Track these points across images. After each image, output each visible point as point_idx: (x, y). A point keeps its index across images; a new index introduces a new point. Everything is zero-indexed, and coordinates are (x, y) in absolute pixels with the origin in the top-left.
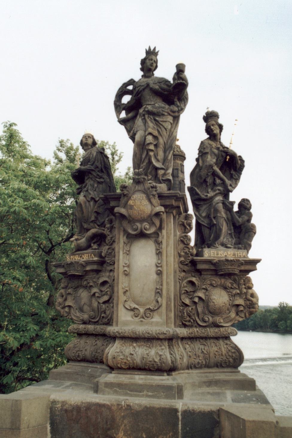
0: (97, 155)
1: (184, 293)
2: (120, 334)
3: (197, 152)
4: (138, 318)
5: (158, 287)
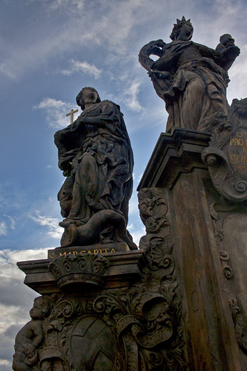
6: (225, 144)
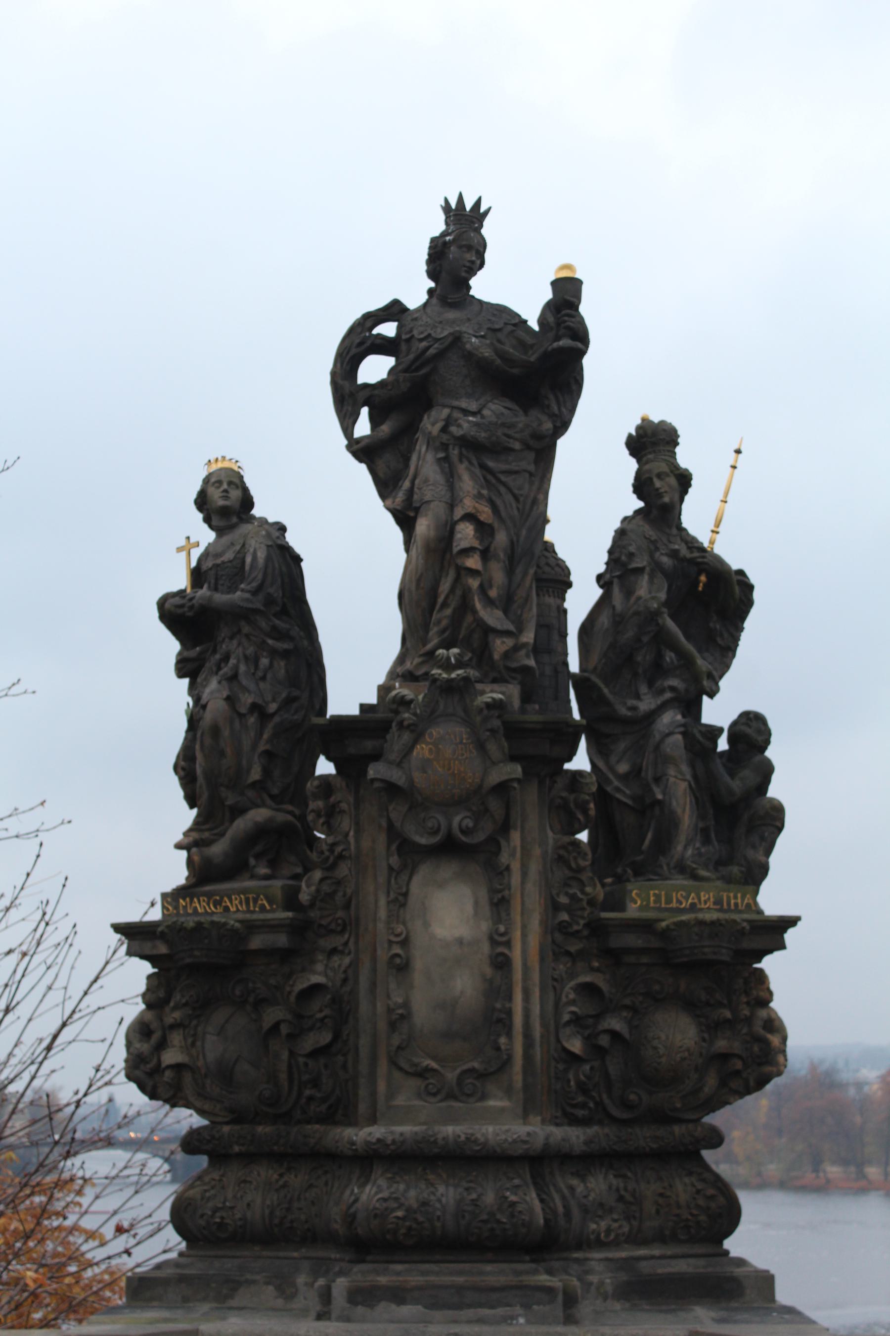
0: (268, 559)
1: (568, 1023)
2: (388, 1145)
3: (605, 557)
4: (439, 1097)
5: (498, 1005)
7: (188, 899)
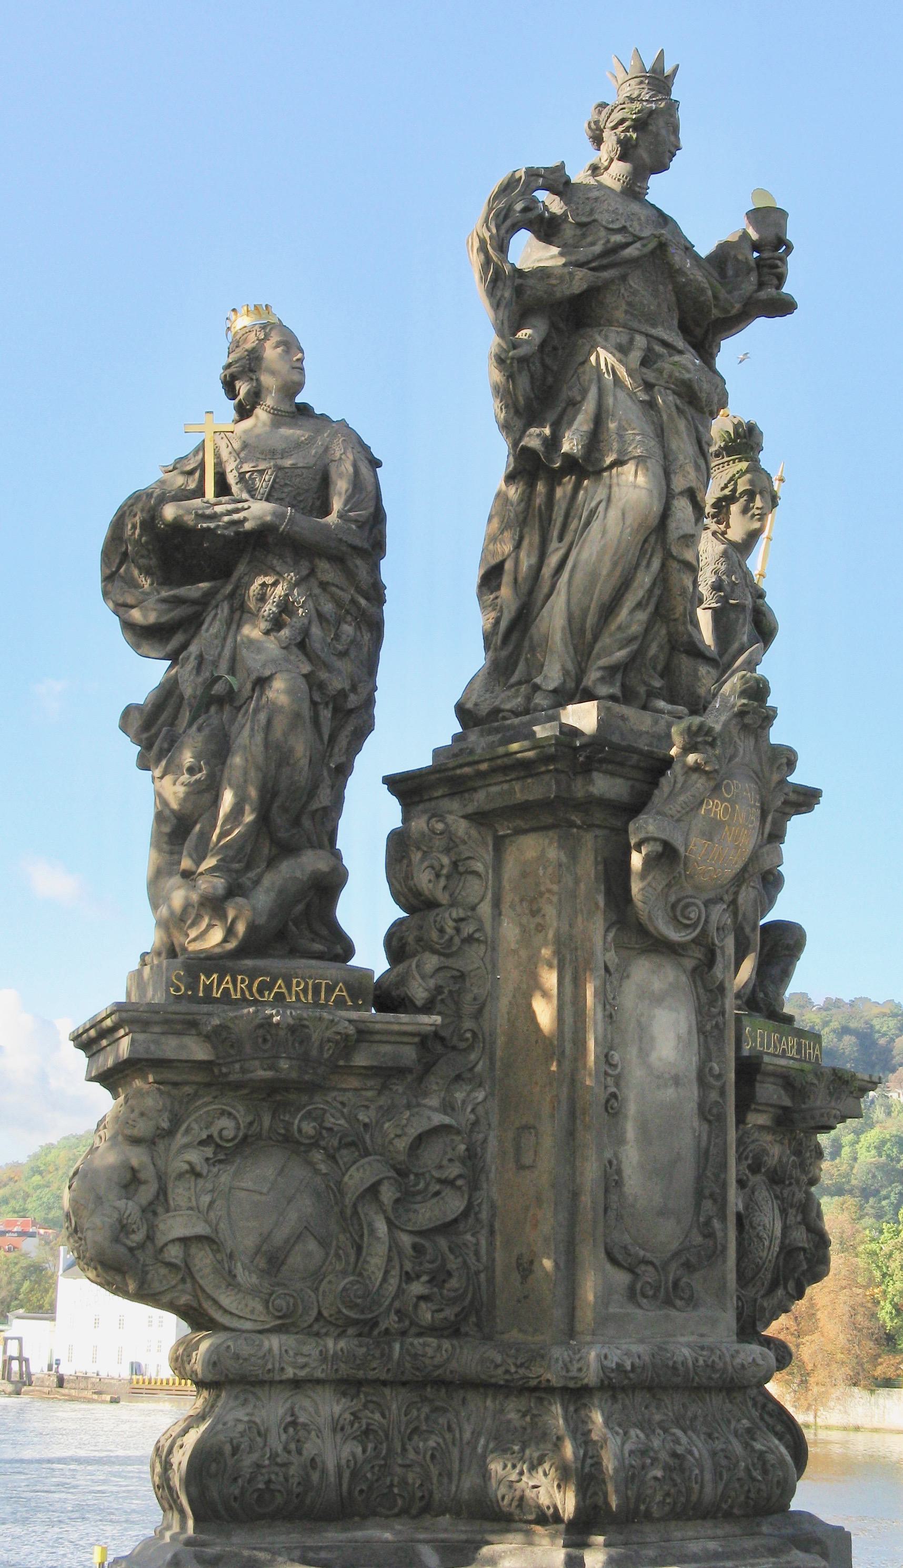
6: (692, 810)
7: (215, 976)
